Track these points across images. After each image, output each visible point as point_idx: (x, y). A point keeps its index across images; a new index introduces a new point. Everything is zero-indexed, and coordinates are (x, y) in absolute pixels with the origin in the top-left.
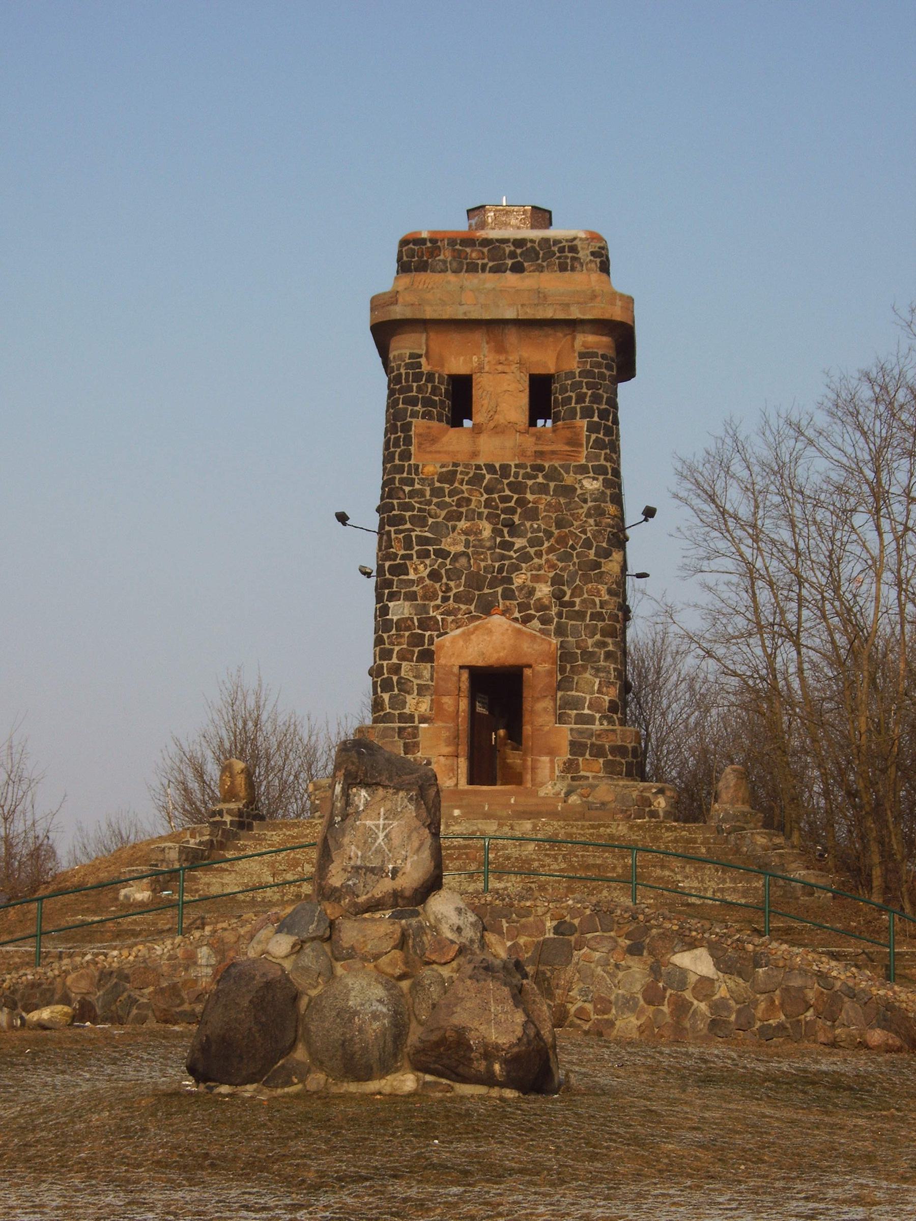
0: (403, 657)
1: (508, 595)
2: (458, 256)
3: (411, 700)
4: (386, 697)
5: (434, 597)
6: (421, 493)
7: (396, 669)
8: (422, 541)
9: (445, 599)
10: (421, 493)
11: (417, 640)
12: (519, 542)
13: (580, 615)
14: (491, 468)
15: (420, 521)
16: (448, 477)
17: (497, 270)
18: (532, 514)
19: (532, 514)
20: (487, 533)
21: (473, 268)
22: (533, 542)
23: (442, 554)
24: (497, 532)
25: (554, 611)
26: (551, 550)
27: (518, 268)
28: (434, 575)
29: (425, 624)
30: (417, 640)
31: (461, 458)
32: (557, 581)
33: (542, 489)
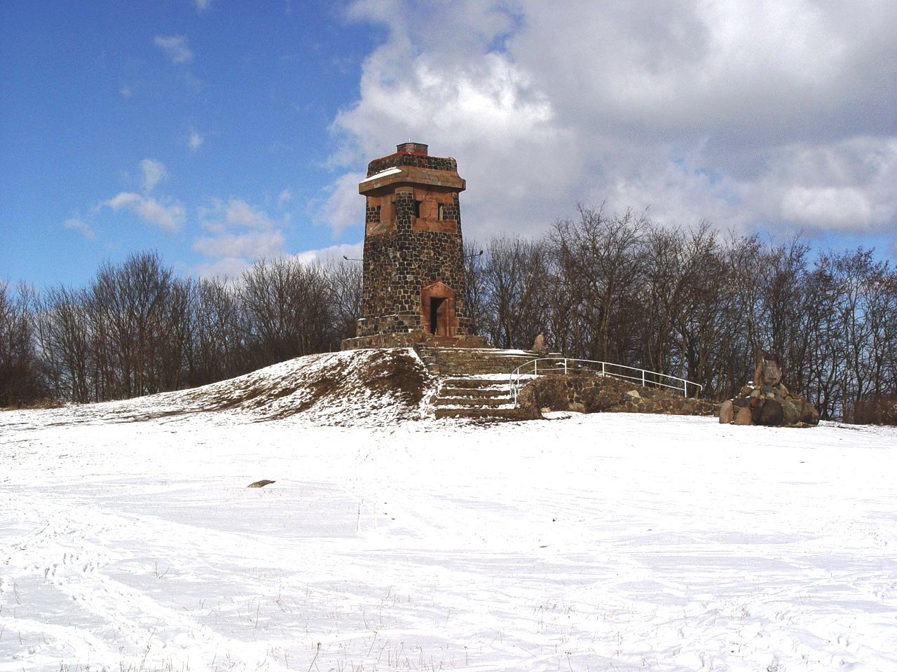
0: (412, 293)
1: (439, 275)
2: (420, 162)
3: (414, 307)
4: (407, 306)
5: (419, 274)
6: (414, 240)
7: (409, 297)
8: (415, 255)
9: (422, 275)
10: (414, 240)
11: (415, 288)
12: (441, 258)
13: (457, 282)
14: (432, 233)
15: (414, 249)
16: (421, 235)
17: (430, 168)
18: (444, 249)
19: (444, 249)
20: (432, 255)
21: (424, 166)
22: (445, 258)
23: (421, 260)
24: (435, 254)
25: (451, 281)
26: (449, 261)
27: (436, 168)
28: (419, 267)
29: (418, 283)
30: (415, 288)
31: (425, 229)
32: (451, 271)
33: (446, 241)
